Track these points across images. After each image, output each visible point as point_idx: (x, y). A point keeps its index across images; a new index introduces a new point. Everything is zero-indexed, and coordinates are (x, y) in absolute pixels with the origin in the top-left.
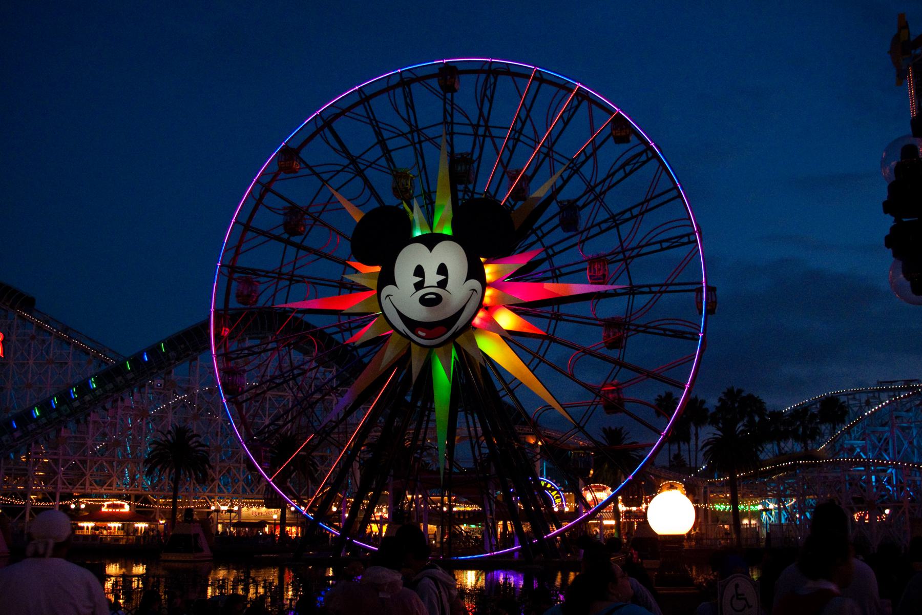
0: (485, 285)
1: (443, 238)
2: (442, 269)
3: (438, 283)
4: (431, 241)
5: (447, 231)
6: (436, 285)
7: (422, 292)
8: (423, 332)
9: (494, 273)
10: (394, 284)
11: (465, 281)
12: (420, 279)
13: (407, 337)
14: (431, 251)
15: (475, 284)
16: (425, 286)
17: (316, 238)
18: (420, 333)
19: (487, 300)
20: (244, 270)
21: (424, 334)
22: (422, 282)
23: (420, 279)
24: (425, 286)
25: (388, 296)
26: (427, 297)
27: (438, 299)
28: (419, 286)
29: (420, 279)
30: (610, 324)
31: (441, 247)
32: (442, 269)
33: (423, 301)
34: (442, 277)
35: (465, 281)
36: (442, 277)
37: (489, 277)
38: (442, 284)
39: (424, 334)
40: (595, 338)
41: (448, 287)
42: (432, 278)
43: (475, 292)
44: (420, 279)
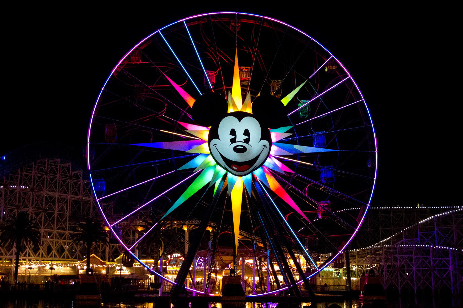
0: (271, 143)
1: (246, 115)
2: (247, 133)
3: (244, 140)
4: (240, 116)
5: (249, 110)
7: (235, 144)
9: (276, 137)
10: (219, 139)
11: (260, 140)
12: (234, 137)
14: (240, 121)
15: (265, 142)
16: (236, 141)
18: (234, 167)
19: (272, 153)
21: (236, 169)
22: (235, 139)
23: (234, 137)
24: (236, 141)
25: (215, 145)
26: (237, 148)
27: (244, 150)
28: (233, 141)
32: (247, 133)
33: (235, 149)
34: (247, 137)
35: (260, 140)
36: (247, 137)
37: (274, 139)
38: (247, 141)
39: (236, 169)
42: (241, 137)
43: (265, 147)
44: (234, 137)
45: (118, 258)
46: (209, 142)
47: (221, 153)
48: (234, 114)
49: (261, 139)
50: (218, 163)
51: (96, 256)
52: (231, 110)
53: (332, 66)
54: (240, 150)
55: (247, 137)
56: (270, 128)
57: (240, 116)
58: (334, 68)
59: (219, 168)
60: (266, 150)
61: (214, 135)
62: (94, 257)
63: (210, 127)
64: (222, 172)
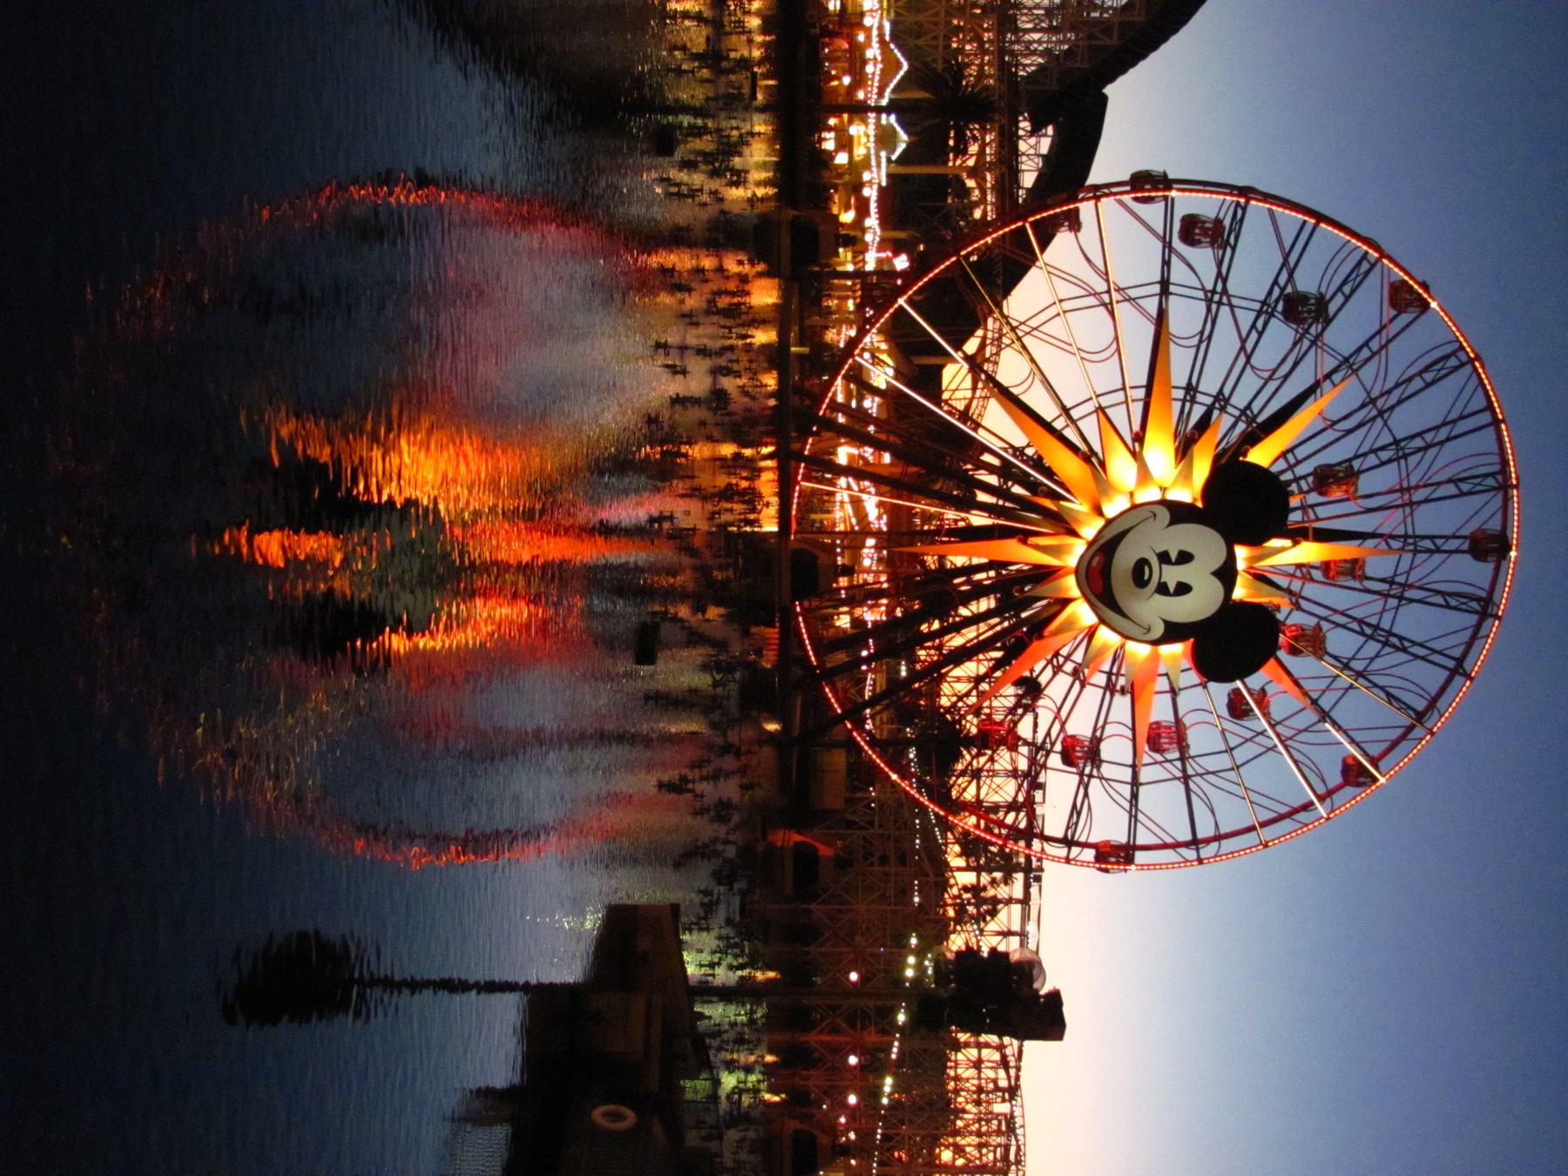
2: (1183, 589)
3: (1165, 583)
5: (1239, 593)
6: (1162, 580)
7: (1154, 562)
8: (1099, 562)
10: (1173, 522)
14: (1217, 574)
15: (1159, 630)
16: (1164, 566)
17: (1280, 335)
18: (1096, 560)
19: (1131, 646)
20: (1238, 222)
23: (1173, 556)
25: (1155, 515)
28: (1164, 558)
29: (1173, 556)
30: (1096, 741)
31: (1217, 587)
33: (1142, 563)
34: (1172, 587)
36: (1172, 587)
38: (1162, 589)
39: (1095, 563)
40: (1080, 726)
45: (898, 129)
46: (1163, 502)
47: (1133, 531)
48: (1231, 558)
50: (1109, 522)
51: (902, 73)
52: (1242, 552)
54: (1139, 573)
56: (1193, 643)
57: (1226, 574)
59: (1100, 523)
61: (1179, 513)
62: (899, 66)
63: (1200, 504)
64: (1091, 529)
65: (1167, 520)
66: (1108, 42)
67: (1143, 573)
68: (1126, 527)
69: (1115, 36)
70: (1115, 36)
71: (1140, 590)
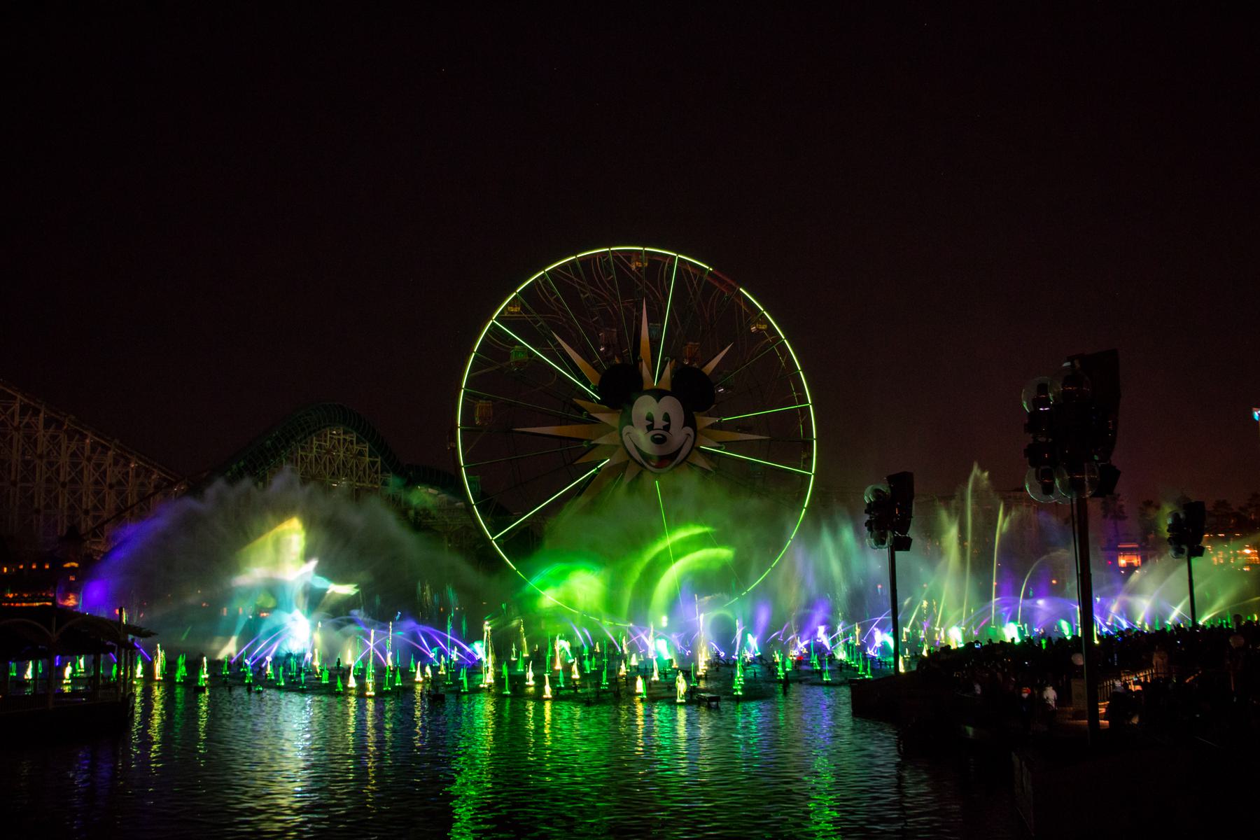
4: (658, 394)
5: (669, 389)
7: (653, 433)
13: (642, 465)
14: (658, 401)
15: (689, 430)
16: (655, 427)
22: (653, 425)
23: (650, 423)
26: (656, 437)
29: (650, 423)
32: (667, 417)
36: (667, 423)
38: (667, 428)
41: (670, 431)
42: (659, 422)
49: (684, 426)
52: (646, 387)
53: (762, 324)
55: (667, 423)
58: (763, 328)
60: (691, 440)
65: (631, 427)
66: (379, 463)
67: (657, 438)
68: (633, 446)
69: (376, 460)
70: (376, 460)
71: (666, 443)
